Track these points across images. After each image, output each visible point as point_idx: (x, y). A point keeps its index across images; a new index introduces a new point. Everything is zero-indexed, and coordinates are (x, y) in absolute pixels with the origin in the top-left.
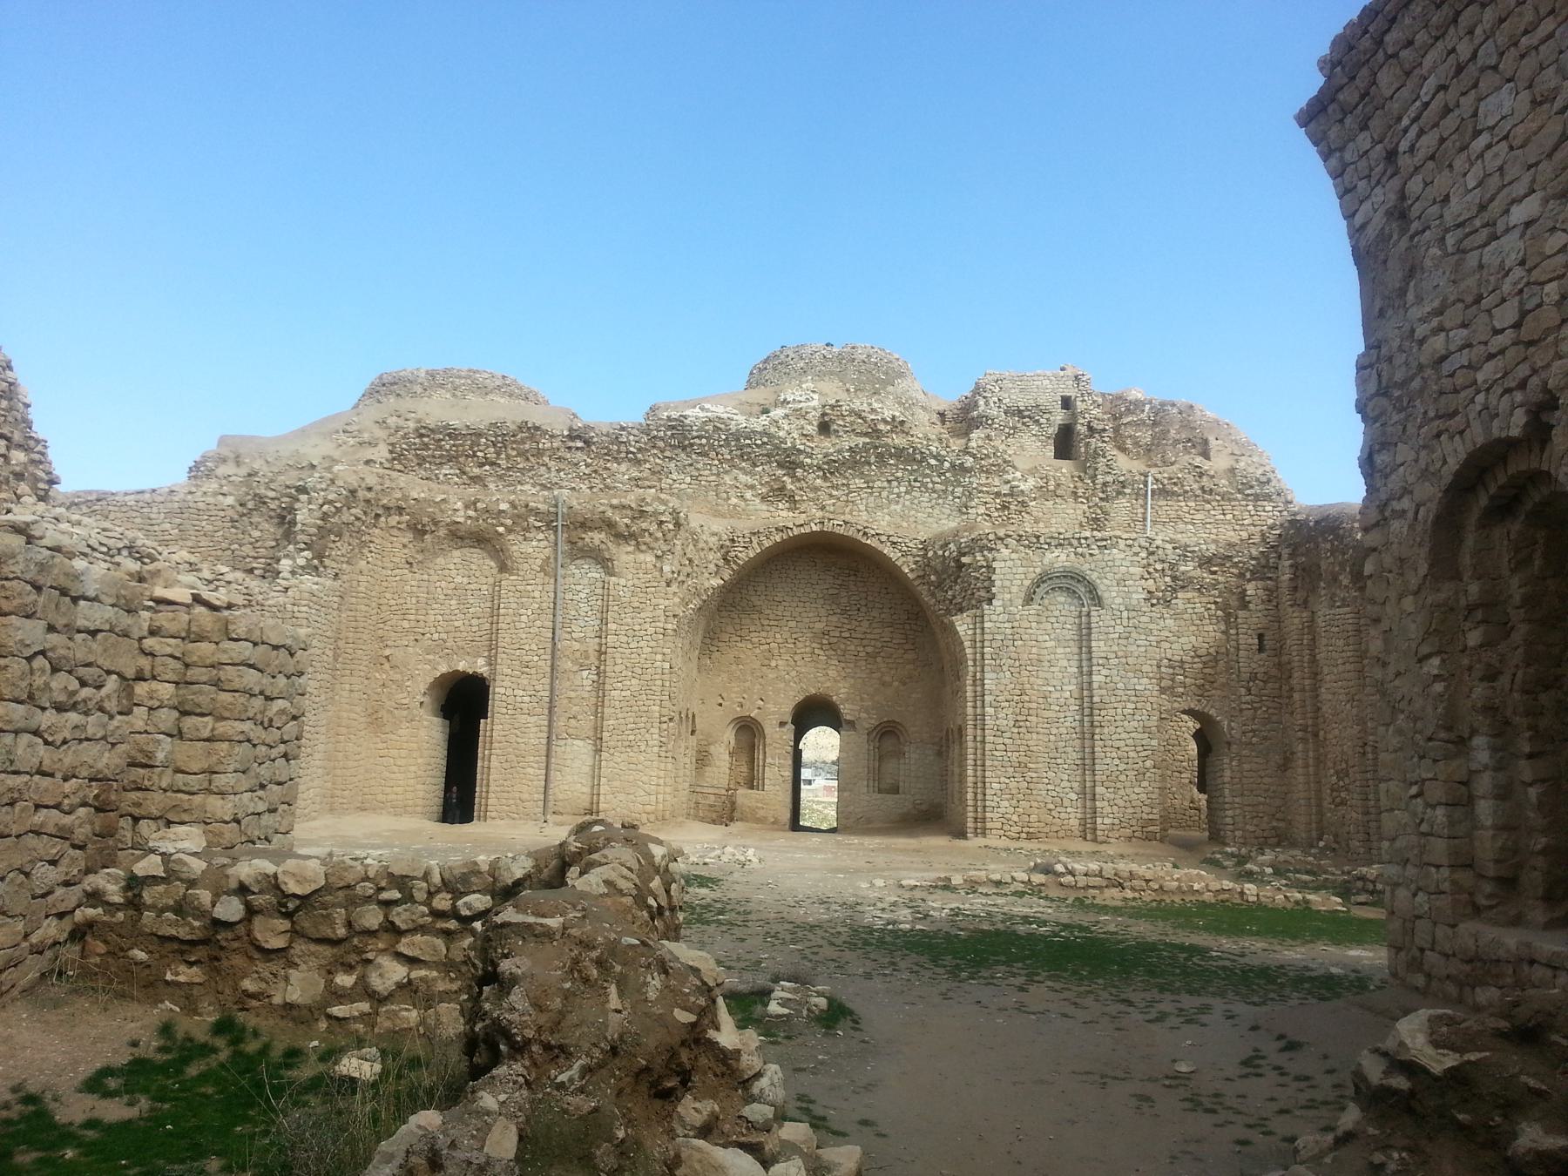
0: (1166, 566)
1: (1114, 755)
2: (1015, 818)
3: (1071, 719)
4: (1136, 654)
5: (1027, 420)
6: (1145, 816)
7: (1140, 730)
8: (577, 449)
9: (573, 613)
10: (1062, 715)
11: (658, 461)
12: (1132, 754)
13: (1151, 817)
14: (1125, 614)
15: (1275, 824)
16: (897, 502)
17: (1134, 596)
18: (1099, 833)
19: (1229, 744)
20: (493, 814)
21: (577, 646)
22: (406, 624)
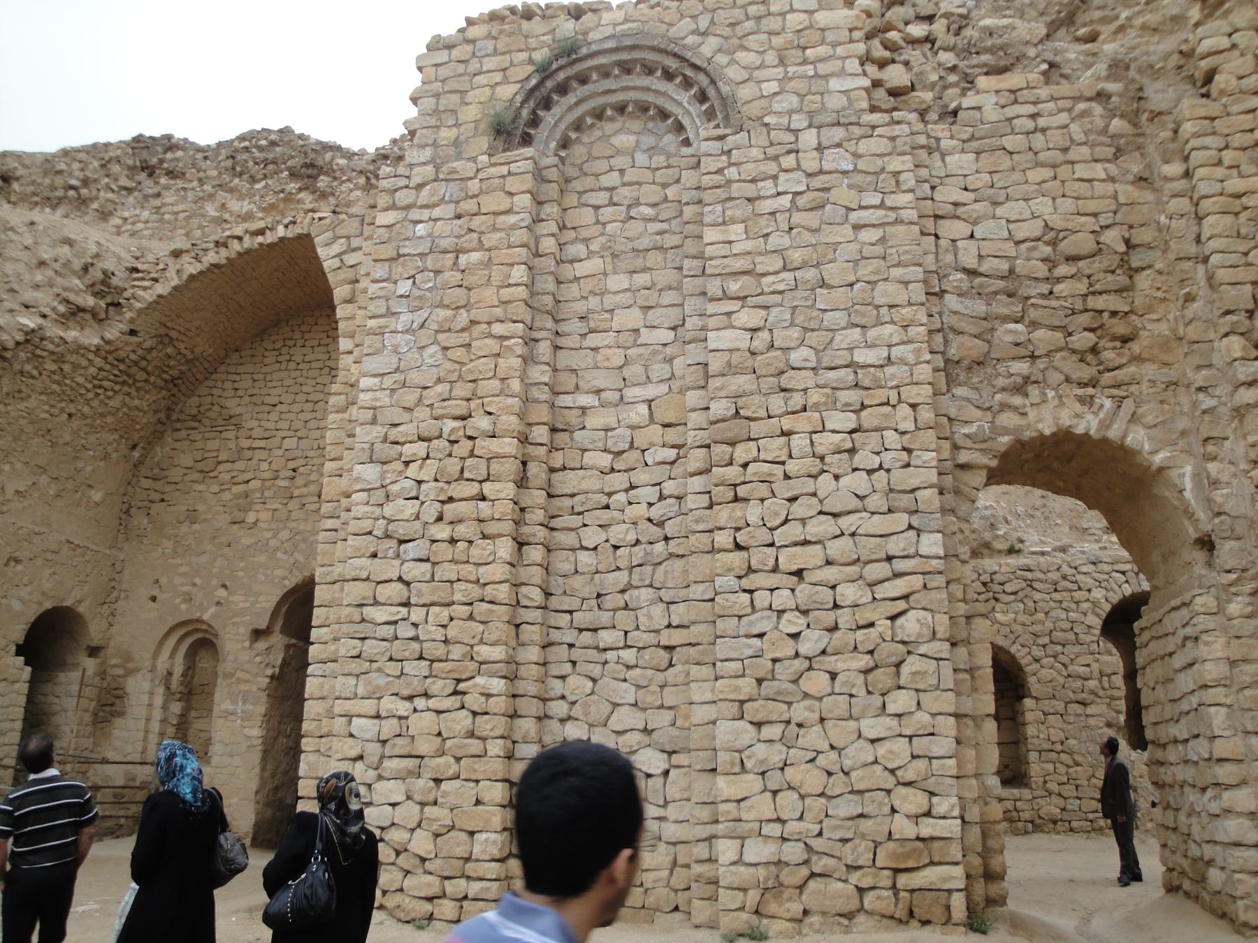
1: (782, 598)
3: (650, 494)
4: (850, 251)
6: (904, 827)
10: (619, 481)
11: (110, 195)
12: (848, 593)
13: (928, 828)
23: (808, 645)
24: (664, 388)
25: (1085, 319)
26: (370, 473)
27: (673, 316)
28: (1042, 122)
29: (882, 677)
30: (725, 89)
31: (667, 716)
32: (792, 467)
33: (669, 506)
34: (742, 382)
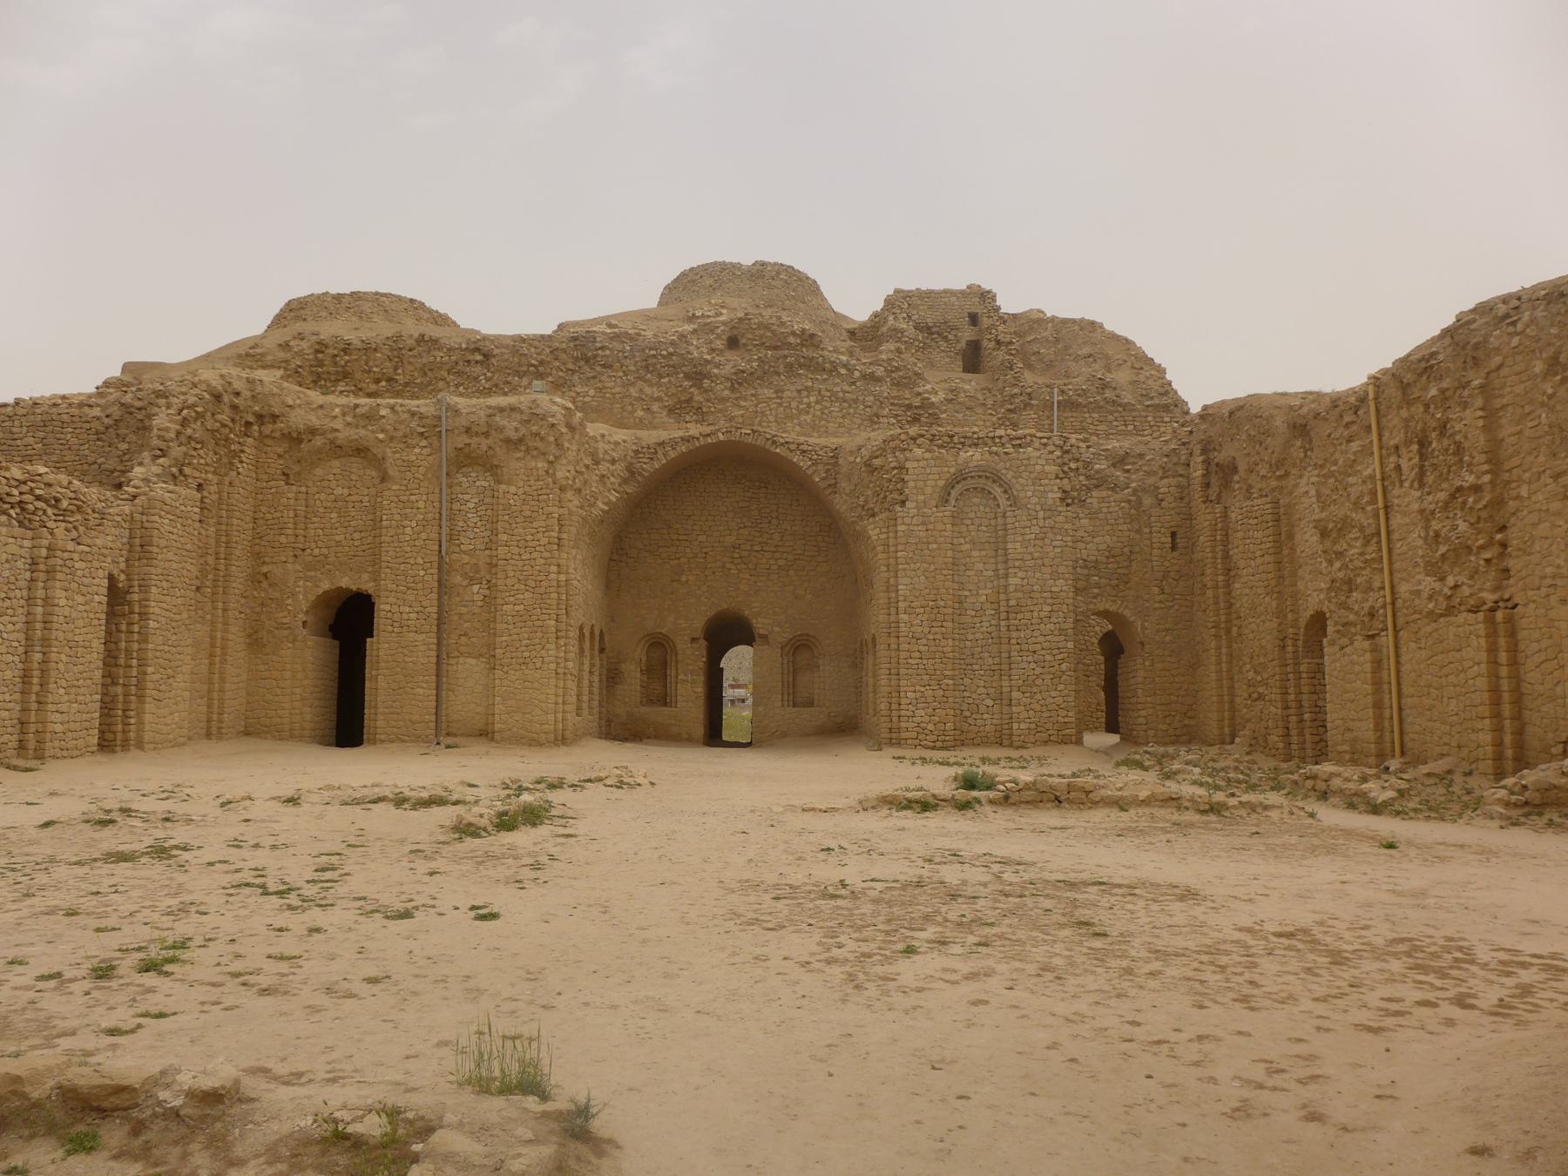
0: (1080, 464)
1: (1030, 658)
2: (930, 727)
3: (987, 624)
4: (1052, 555)
5: (936, 336)
7: (1056, 632)
8: (477, 362)
9: (461, 524)
10: (978, 620)
11: (560, 373)
12: (1048, 658)
15: (1186, 722)
16: (808, 413)
17: (1050, 495)
18: (1015, 738)
19: (1142, 644)
20: (383, 737)
21: (466, 559)
22: (283, 539)
26: (904, 617)
27: (994, 567)
28: (1111, 510)
30: (1015, 493)
32: (1033, 621)
33: (993, 628)
34: (1020, 595)
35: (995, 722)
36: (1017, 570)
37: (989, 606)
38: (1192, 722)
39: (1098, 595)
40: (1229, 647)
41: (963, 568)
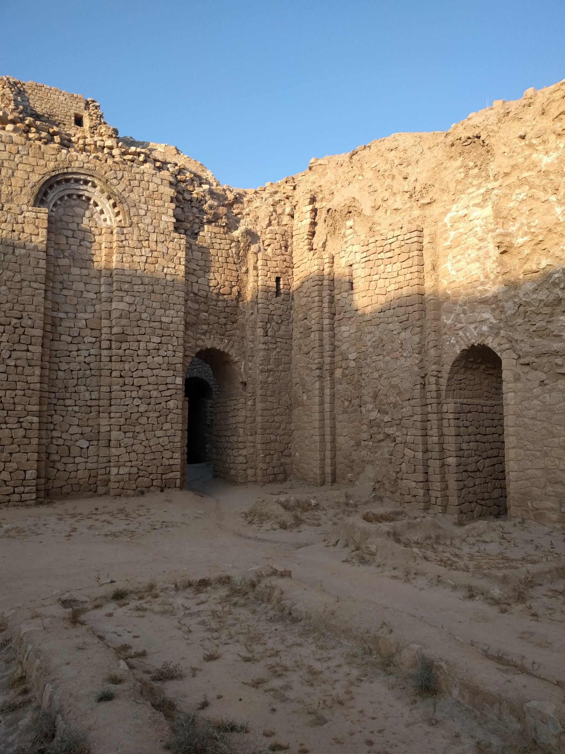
1: (134, 394)
7: (164, 366)
10: (74, 347)
12: (155, 394)
13: (171, 462)
14: (153, 237)
15: (283, 460)
19: (245, 384)
23: (142, 409)
24: (91, 316)
25: (224, 315)
29: (162, 419)
31: (90, 429)
32: (140, 352)
33: (92, 358)
34: (124, 322)
35: (90, 466)
36: (122, 294)
37: (88, 331)
38: (288, 460)
39: (206, 331)
40: (332, 388)
41: (59, 286)
